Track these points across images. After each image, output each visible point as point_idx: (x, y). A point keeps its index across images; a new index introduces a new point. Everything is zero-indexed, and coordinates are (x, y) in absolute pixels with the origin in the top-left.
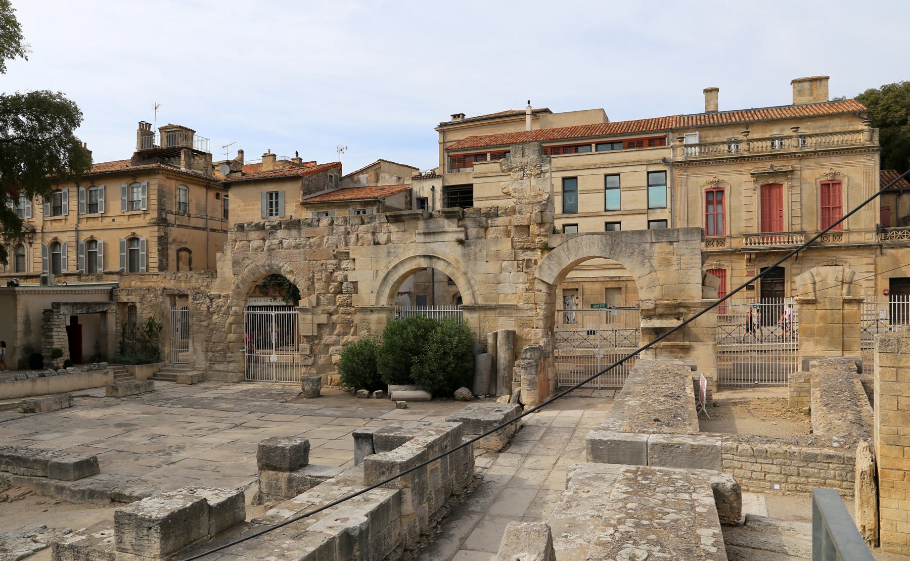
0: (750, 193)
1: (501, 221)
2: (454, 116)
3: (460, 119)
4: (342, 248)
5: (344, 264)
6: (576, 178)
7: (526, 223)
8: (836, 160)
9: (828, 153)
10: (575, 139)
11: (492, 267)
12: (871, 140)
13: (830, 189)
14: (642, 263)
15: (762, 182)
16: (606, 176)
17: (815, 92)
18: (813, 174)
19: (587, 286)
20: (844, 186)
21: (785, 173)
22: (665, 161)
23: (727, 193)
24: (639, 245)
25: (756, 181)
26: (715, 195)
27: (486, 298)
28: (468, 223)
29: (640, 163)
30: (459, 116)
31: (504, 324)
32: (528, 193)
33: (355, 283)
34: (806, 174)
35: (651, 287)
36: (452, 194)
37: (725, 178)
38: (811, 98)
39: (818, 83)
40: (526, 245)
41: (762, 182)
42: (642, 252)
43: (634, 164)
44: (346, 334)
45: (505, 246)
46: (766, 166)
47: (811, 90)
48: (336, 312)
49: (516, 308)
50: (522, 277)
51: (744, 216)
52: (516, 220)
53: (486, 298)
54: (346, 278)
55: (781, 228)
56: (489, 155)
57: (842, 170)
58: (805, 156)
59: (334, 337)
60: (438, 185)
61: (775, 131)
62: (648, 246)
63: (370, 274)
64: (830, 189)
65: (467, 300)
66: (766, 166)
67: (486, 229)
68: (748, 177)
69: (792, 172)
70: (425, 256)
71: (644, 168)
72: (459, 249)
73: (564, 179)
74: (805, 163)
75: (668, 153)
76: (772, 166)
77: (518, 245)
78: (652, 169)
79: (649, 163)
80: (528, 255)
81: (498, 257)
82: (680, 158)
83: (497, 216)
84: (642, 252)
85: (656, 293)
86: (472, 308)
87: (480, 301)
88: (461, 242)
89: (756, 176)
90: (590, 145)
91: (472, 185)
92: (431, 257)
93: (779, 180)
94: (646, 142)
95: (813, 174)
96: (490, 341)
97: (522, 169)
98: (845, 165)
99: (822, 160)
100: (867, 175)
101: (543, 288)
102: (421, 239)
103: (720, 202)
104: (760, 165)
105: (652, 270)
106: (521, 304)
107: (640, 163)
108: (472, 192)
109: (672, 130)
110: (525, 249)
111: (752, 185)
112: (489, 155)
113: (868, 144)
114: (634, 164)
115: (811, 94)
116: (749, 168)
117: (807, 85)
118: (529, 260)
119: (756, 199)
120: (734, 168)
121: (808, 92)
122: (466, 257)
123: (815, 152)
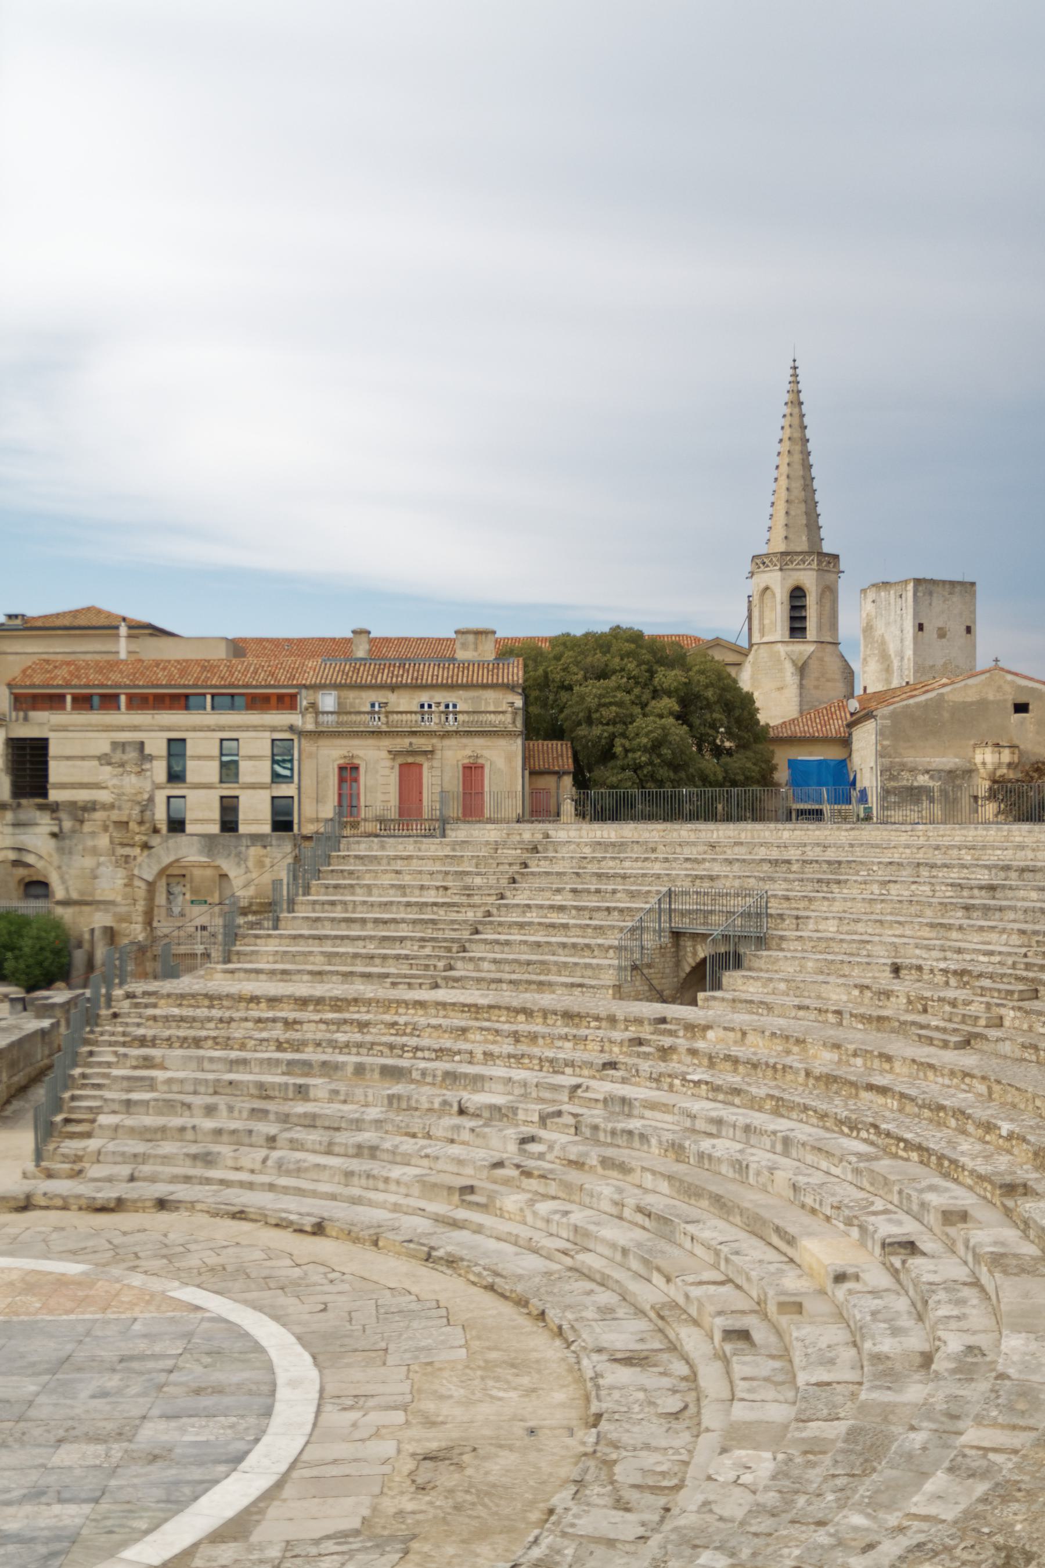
0: (387, 772)
1: (99, 815)
2: (10, 617)
3: (18, 622)
6: (184, 740)
7: (125, 819)
8: (479, 741)
10: (185, 686)
11: (89, 862)
12: (514, 722)
13: (472, 772)
14: (238, 864)
15: (400, 760)
16: (222, 740)
17: (480, 648)
18: (454, 754)
19: (197, 872)
20: (487, 771)
22: (291, 728)
23: (362, 770)
25: (394, 759)
26: (348, 772)
27: (81, 893)
28: (63, 815)
29: (262, 728)
30: (16, 616)
31: (101, 919)
32: (129, 790)
34: (449, 754)
35: (246, 886)
37: (360, 753)
40: (125, 841)
41: (400, 760)
42: (238, 854)
43: (255, 728)
45: (103, 841)
49: (112, 903)
50: (121, 873)
52: (115, 815)
53: (81, 893)
55: (421, 814)
57: (486, 753)
58: (447, 734)
61: (425, 697)
62: (243, 849)
64: (472, 772)
67: (82, 822)
68: (384, 754)
69: (432, 752)
70: (13, 849)
71: (267, 734)
72: (52, 843)
73: (170, 740)
74: (447, 742)
77: (117, 841)
79: (274, 729)
80: (127, 851)
81: (95, 851)
82: (310, 726)
83: (94, 810)
84: (238, 854)
85: (251, 891)
86: (66, 903)
87: (75, 896)
88: (54, 835)
89: (394, 754)
90: (204, 695)
91: (46, 740)
92: (20, 850)
93: (419, 759)
94: (274, 701)
95: (454, 754)
96: (87, 936)
98: (488, 747)
99: (465, 741)
100: (509, 759)
101: (143, 885)
102: (9, 830)
103: (356, 780)
104: (398, 741)
105: (248, 871)
106: (119, 899)
107: (262, 728)
109: (305, 687)
110: (123, 845)
111: (389, 763)
113: (511, 728)
114: (255, 728)
115: (476, 649)
116: (387, 743)
118: (128, 856)
119: (394, 778)
120: (371, 742)
121: (472, 646)
122: (61, 850)
123: (457, 732)
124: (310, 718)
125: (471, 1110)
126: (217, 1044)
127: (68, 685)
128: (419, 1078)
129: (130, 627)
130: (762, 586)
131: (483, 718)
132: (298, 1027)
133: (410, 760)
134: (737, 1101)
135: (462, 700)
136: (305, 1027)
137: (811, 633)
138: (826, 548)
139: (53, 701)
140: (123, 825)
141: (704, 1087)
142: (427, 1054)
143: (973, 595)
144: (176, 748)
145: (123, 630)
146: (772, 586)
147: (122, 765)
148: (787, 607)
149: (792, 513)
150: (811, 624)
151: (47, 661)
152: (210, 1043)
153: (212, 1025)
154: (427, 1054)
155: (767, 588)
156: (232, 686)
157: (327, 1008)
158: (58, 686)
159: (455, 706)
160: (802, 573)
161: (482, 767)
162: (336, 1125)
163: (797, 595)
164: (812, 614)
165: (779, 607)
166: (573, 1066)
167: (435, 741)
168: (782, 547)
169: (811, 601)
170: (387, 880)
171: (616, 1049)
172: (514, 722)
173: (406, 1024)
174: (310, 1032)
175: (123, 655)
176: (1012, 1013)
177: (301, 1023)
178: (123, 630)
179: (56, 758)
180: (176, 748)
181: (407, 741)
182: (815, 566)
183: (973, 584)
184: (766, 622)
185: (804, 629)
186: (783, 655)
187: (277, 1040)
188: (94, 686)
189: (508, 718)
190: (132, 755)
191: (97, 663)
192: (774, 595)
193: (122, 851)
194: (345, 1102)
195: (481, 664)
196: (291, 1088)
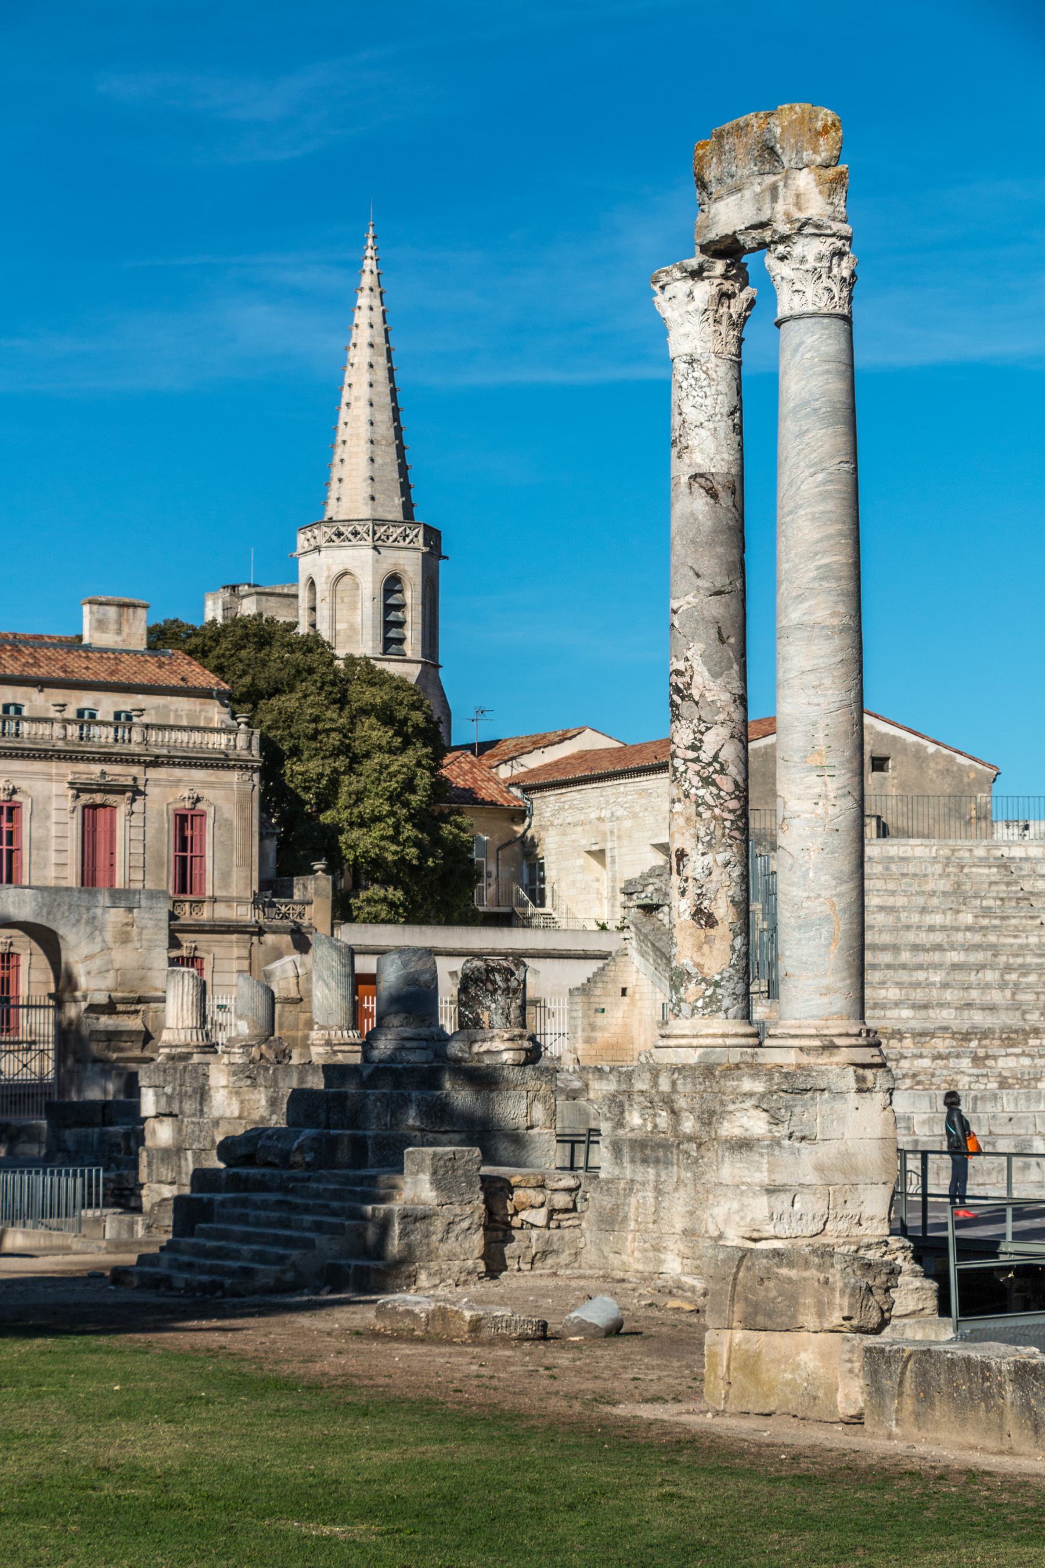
9: (189, 762)
12: (249, 747)
13: (186, 824)
14: (91, 937)
17: (126, 629)
20: (209, 822)
21: (120, 790)
24: (88, 909)
38: (118, 639)
39: (131, 610)
51: (53, 858)
58: (156, 762)
61: (86, 700)
64: (186, 824)
74: (153, 773)
76: (103, 774)
85: (109, 981)
89: (80, 789)
93: (111, 799)
99: (178, 773)
104: (81, 767)
115: (119, 631)
117: (112, 612)
121: (113, 626)
126: (918, 1083)
130: (337, 569)
131: (182, 737)
132: (990, 1063)
133: (98, 798)
136: (1001, 1063)
146: (356, 571)
149: (379, 460)
152: (908, 1082)
157: (997, 1042)
160: (403, 553)
161: (202, 815)
163: (392, 584)
165: (368, 605)
167: (135, 770)
168: (365, 511)
172: (249, 747)
181: (96, 769)
187: (1000, 1075)
192: (357, 586)
195: (118, 653)
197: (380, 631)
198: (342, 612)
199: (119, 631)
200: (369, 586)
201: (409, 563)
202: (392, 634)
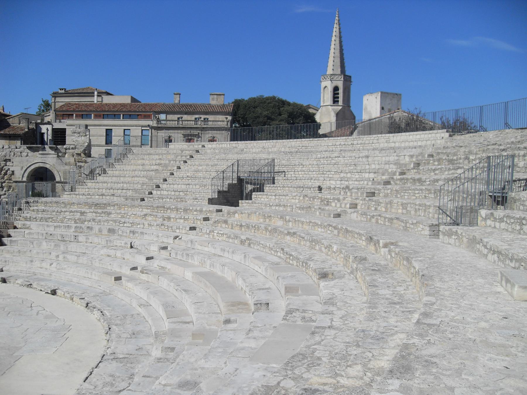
4: (8, 158)
5: (8, 163)
7: (79, 153)
12: (227, 124)
16: (125, 130)
17: (219, 100)
22: (149, 126)
33: (13, 172)
36: (55, 132)
44: (8, 191)
45: (72, 160)
46: (188, 132)
47: (217, 99)
48: (4, 182)
52: (77, 151)
54: (9, 169)
56: (74, 115)
58: (203, 129)
59: (4, 192)
60: (50, 127)
61: (197, 116)
63: (19, 168)
65: (58, 179)
66: (188, 132)
75: (150, 123)
77: (77, 160)
78: (143, 128)
80: (80, 164)
82: (155, 125)
87: (62, 180)
91: (65, 129)
94: (143, 116)
97: (79, 133)
108: (65, 132)
110: (79, 162)
111: (182, 139)
112: (74, 115)
115: (217, 100)
116: (182, 132)
121: (215, 99)
124: (155, 122)
125: (135, 247)
127: (74, 111)
128: (121, 234)
129: (98, 93)
133: (190, 138)
134: (236, 241)
135: (211, 118)
137: (341, 103)
138: (347, 74)
139: (70, 116)
140: (79, 155)
141: (225, 236)
142: (128, 225)
143: (400, 98)
144: (109, 133)
145: (96, 93)
147: (79, 133)
148: (332, 93)
149: (335, 61)
150: (341, 100)
151: (70, 104)
153: (54, 213)
154: (128, 225)
155: (326, 87)
156: (130, 111)
158: (71, 111)
159: (208, 119)
162: (84, 252)
163: (336, 89)
164: (341, 96)
165: (330, 93)
166: (179, 229)
169: (341, 91)
170: (140, 162)
171: (199, 222)
172: (227, 124)
173: (124, 214)
174: (90, 216)
175: (96, 102)
176: (361, 202)
177: (87, 213)
178: (96, 93)
179: (94, 146)
180: (109, 133)
182: (342, 79)
183: (400, 95)
184: (325, 98)
185: (338, 101)
186: (331, 109)
188: (83, 111)
189: (225, 123)
190: (83, 129)
191: (86, 104)
193: (78, 164)
194: (91, 243)
196: (73, 237)
197: (332, 99)
198: (325, 95)
199: (217, 100)
200: (330, 89)
201: (340, 84)
202: (336, 100)
